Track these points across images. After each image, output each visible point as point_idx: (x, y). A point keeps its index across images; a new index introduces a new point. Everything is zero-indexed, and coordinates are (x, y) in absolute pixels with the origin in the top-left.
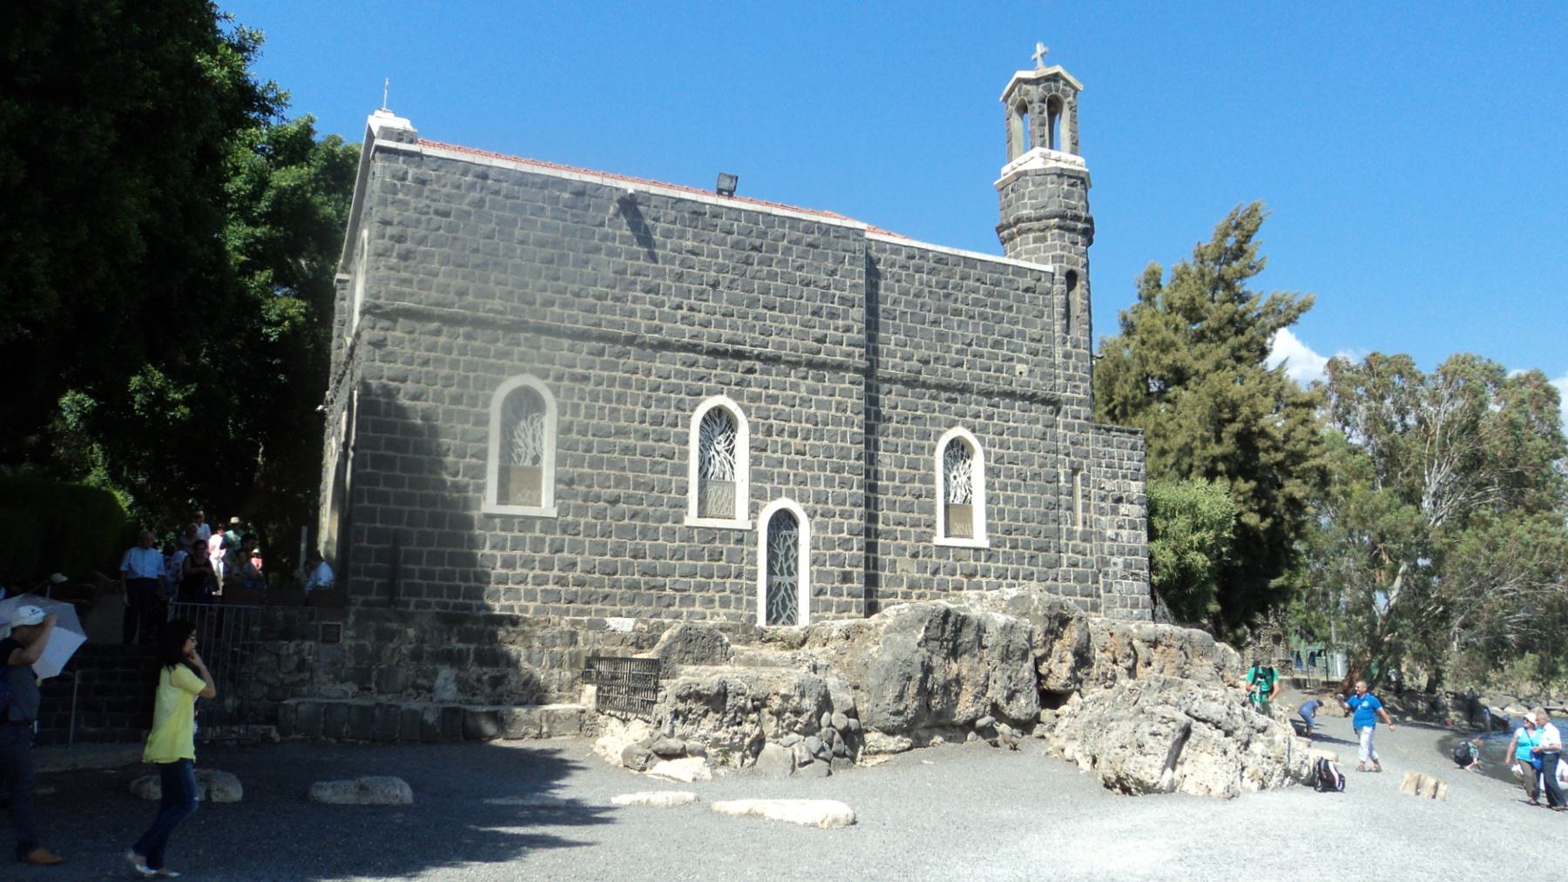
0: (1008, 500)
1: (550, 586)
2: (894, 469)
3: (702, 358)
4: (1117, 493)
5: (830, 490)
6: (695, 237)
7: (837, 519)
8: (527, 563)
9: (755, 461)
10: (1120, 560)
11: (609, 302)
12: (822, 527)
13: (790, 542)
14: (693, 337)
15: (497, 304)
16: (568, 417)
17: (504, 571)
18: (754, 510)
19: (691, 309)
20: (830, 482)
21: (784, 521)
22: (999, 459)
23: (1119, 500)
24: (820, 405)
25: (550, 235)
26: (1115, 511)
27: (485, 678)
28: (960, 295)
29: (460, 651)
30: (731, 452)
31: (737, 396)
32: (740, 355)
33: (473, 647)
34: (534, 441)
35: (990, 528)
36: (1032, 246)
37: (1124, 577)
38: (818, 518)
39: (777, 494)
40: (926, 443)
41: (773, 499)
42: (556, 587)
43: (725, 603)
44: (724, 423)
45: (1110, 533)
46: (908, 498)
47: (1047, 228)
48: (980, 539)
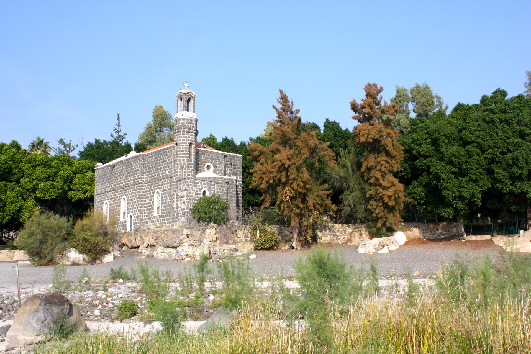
10: (181, 212)
12: (135, 217)
23: (181, 197)
26: (181, 200)
31: (126, 195)
35: (162, 210)
37: (182, 216)
48: (160, 214)
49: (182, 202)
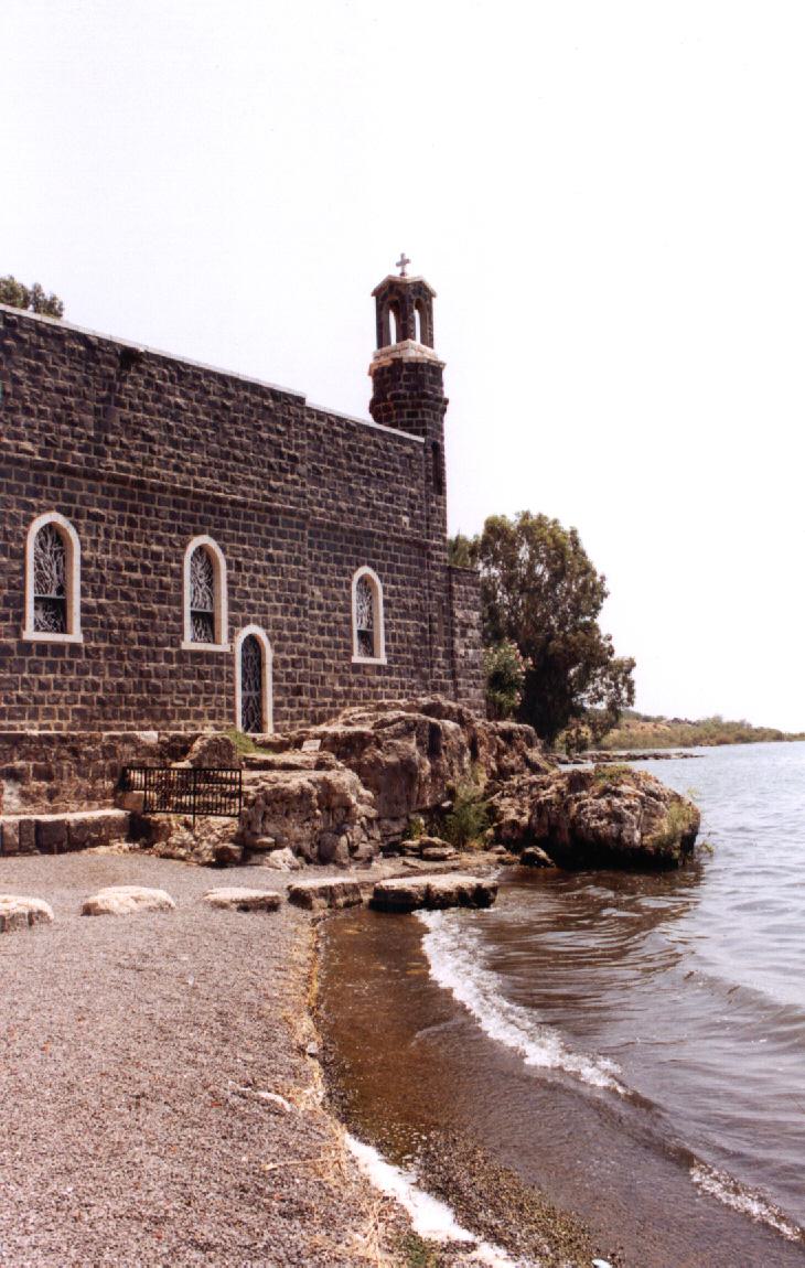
0: (399, 626)
1: (78, 706)
2: (322, 600)
3: (189, 500)
4: (465, 621)
5: (285, 618)
6: (184, 395)
7: (290, 643)
8: (58, 686)
9: (231, 592)
11: (118, 449)
12: (278, 649)
13: (255, 663)
14: (184, 483)
15: (27, 445)
16: (88, 554)
17: (41, 693)
18: (232, 635)
20: (285, 611)
22: (392, 594)
25: (66, 384)
26: (464, 634)
27: (44, 790)
28: (364, 458)
29: (22, 769)
30: (210, 584)
31: (215, 536)
33: (31, 764)
34: (58, 573)
35: (387, 649)
36: (406, 419)
38: (276, 642)
39: (246, 622)
40: (343, 579)
41: (244, 626)
42: (84, 707)
43: (212, 717)
44: (205, 559)
45: (462, 651)
46: (333, 624)
47: (419, 405)
48: (382, 660)
49: (466, 640)
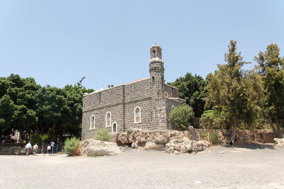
4: (160, 110)
9: (112, 118)
12: (118, 124)
18: (112, 124)
19: (106, 102)
21: (115, 125)
23: (161, 110)
24: (118, 109)
32: (110, 106)
35: (141, 120)
38: (118, 123)
